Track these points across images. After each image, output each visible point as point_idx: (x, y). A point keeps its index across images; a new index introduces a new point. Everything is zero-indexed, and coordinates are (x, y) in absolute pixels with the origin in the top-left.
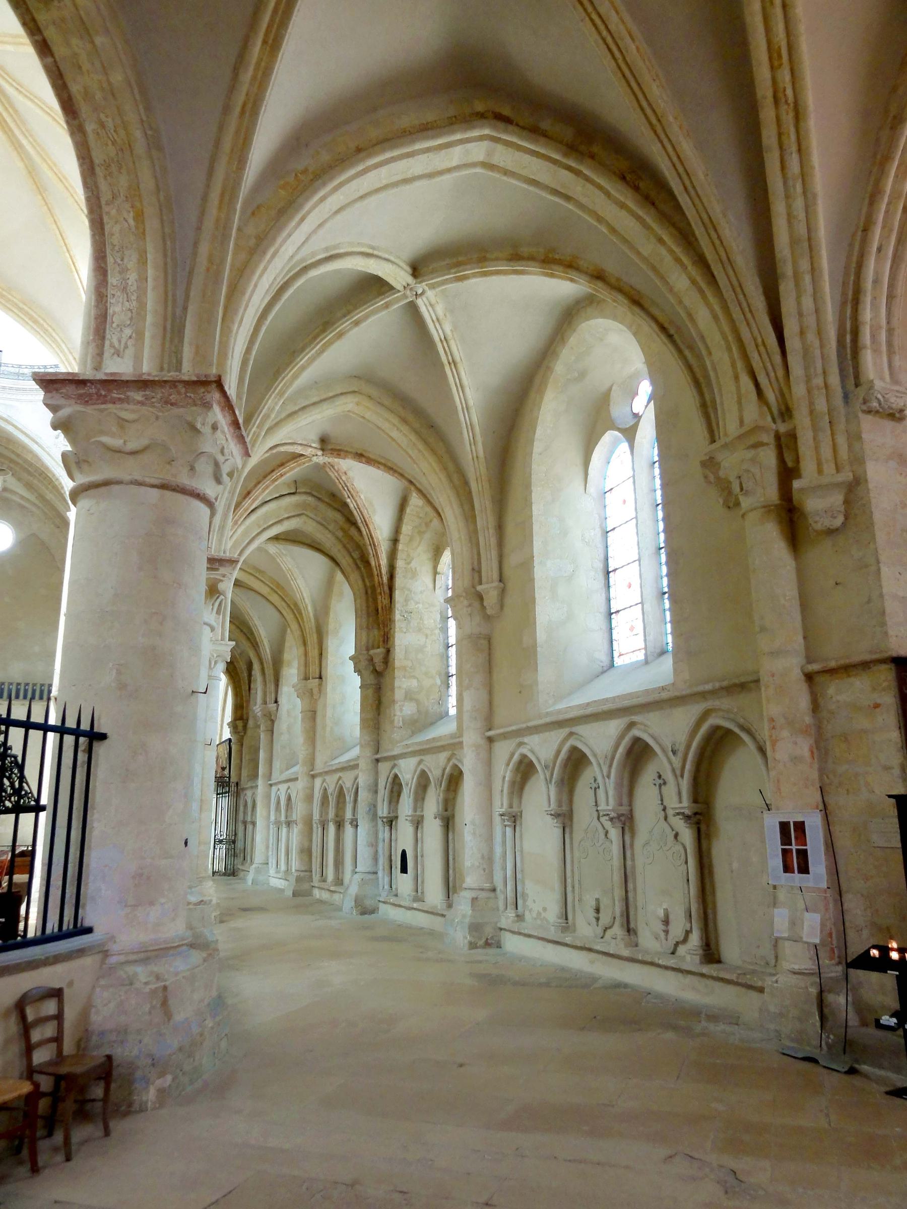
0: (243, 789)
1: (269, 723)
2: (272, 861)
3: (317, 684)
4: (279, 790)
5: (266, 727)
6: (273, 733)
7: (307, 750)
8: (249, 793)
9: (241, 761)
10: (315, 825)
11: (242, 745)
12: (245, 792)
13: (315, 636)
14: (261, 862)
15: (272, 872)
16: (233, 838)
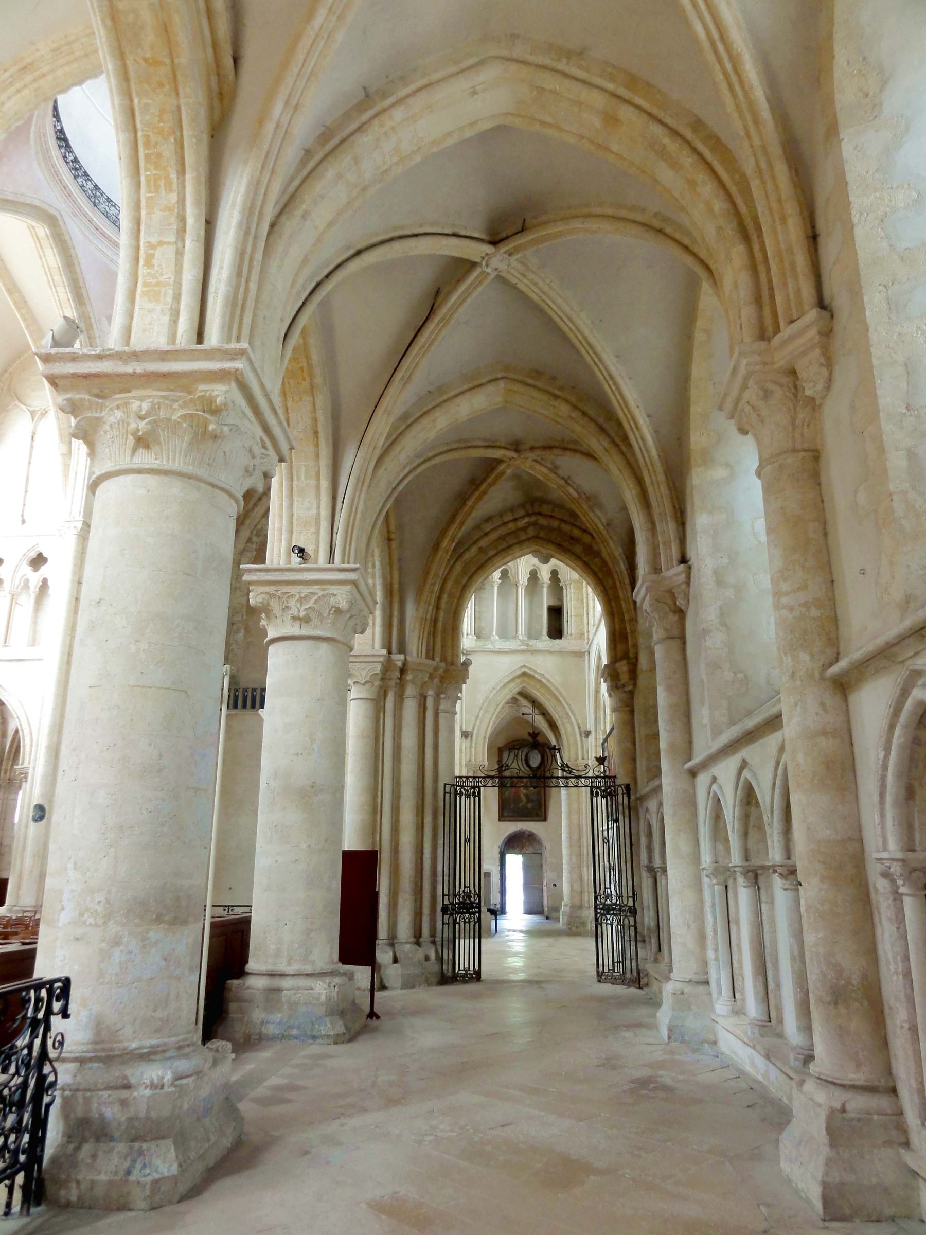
0: (642, 799)
1: (673, 618)
2: (719, 976)
3: (813, 333)
4: (714, 779)
5: (666, 630)
6: (684, 643)
7: (804, 587)
8: (652, 804)
9: (634, 743)
10: (880, 885)
11: (632, 712)
12: (645, 804)
13: (782, 171)
14: (688, 977)
15: (721, 1006)
16: (631, 903)
